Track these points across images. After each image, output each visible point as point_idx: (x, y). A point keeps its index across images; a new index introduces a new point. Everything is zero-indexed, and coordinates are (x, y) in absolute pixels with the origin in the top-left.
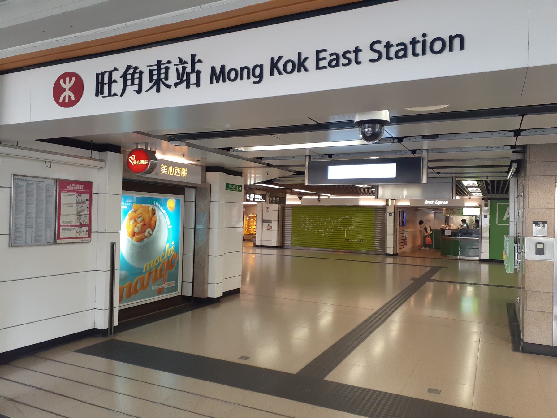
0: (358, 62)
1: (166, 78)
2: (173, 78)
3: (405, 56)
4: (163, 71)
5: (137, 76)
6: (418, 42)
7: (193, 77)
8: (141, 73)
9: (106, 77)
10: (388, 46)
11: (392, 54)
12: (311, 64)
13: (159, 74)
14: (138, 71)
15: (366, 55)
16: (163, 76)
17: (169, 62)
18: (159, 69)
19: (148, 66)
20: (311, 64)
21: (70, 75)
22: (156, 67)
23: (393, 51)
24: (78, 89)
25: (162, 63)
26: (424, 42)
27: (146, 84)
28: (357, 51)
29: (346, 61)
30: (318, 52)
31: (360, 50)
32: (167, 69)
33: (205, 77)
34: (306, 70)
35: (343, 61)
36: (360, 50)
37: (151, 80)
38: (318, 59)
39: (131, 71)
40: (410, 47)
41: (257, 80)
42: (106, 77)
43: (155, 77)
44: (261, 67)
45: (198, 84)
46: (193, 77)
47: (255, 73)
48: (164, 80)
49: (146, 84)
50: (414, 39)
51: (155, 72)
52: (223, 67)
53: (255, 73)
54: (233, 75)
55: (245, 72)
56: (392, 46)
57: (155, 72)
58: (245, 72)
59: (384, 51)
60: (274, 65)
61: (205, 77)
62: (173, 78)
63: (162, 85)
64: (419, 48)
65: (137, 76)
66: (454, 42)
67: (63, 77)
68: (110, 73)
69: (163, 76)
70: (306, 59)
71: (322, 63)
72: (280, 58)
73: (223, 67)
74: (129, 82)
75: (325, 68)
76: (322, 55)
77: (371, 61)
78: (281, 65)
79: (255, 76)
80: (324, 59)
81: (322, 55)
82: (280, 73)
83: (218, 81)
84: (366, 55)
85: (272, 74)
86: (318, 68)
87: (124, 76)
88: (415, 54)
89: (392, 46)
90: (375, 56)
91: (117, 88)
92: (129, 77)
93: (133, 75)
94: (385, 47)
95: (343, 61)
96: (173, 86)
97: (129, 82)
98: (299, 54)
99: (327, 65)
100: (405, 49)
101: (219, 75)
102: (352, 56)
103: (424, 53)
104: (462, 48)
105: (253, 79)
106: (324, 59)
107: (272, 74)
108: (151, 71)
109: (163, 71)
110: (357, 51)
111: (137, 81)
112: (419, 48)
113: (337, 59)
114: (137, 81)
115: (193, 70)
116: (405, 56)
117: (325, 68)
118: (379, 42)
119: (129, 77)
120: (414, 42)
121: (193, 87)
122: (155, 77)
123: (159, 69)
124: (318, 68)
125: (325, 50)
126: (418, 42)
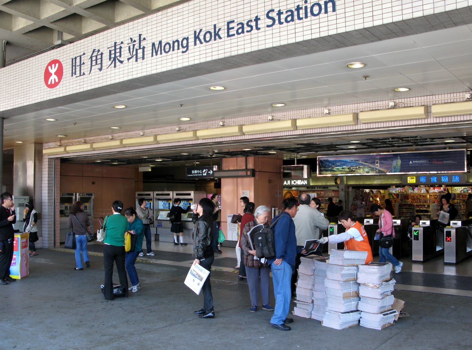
0: (258, 29)
1: (120, 56)
3: (292, 20)
4: (118, 51)
5: (99, 57)
6: (302, 8)
8: (102, 54)
9: (78, 60)
10: (280, 13)
11: (283, 20)
13: (115, 53)
14: (100, 53)
15: (264, 22)
16: (118, 54)
17: (122, 43)
18: (115, 50)
19: (108, 48)
22: (113, 48)
23: (283, 17)
25: (117, 44)
26: (306, 8)
27: (106, 61)
28: (257, 19)
29: (249, 29)
30: (228, 23)
31: (259, 19)
32: (121, 48)
34: (220, 38)
35: (247, 28)
36: (259, 19)
37: (110, 59)
38: (229, 29)
39: (95, 54)
40: (295, 13)
41: (185, 49)
42: (78, 60)
43: (113, 56)
44: (187, 39)
45: (143, 58)
46: (140, 52)
48: (118, 58)
49: (106, 61)
50: (298, 6)
51: (113, 52)
52: (160, 43)
55: (176, 44)
56: (282, 13)
57: (113, 52)
58: (176, 44)
59: (276, 18)
60: (196, 37)
63: (117, 61)
64: (302, 12)
65: (99, 57)
68: (80, 56)
69: (118, 54)
70: (219, 30)
71: (232, 32)
72: (201, 30)
73: (160, 43)
75: (234, 35)
76: (231, 25)
77: (268, 26)
78: (201, 37)
79: (183, 47)
80: (233, 28)
81: (231, 25)
82: (201, 43)
83: (156, 54)
84: (264, 22)
85: (195, 44)
86: (229, 36)
87: (91, 57)
88: (299, 18)
89: (282, 13)
90: (270, 22)
92: (94, 58)
93: (96, 56)
94: (277, 14)
95: (247, 28)
96: (126, 61)
98: (215, 26)
99: (236, 33)
100: (292, 15)
101: (158, 48)
102: (253, 24)
103: (306, 17)
104: (334, 10)
105: (181, 49)
106: (233, 28)
107: (195, 44)
108: (110, 51)
109: (118, 51)
110: (257, 19)
112: (302, 12)
113: (243, 28)
115: (140, 48)
116: (292, 20)
117: (234, 35)
118: (273, 11)
119: (94, 58)
120: (298, 8)
121: (140, 60)
122: (113, 56)
123: (115, 50)
124: (229, 36)
125: (233, 22)
126: (302, 8)
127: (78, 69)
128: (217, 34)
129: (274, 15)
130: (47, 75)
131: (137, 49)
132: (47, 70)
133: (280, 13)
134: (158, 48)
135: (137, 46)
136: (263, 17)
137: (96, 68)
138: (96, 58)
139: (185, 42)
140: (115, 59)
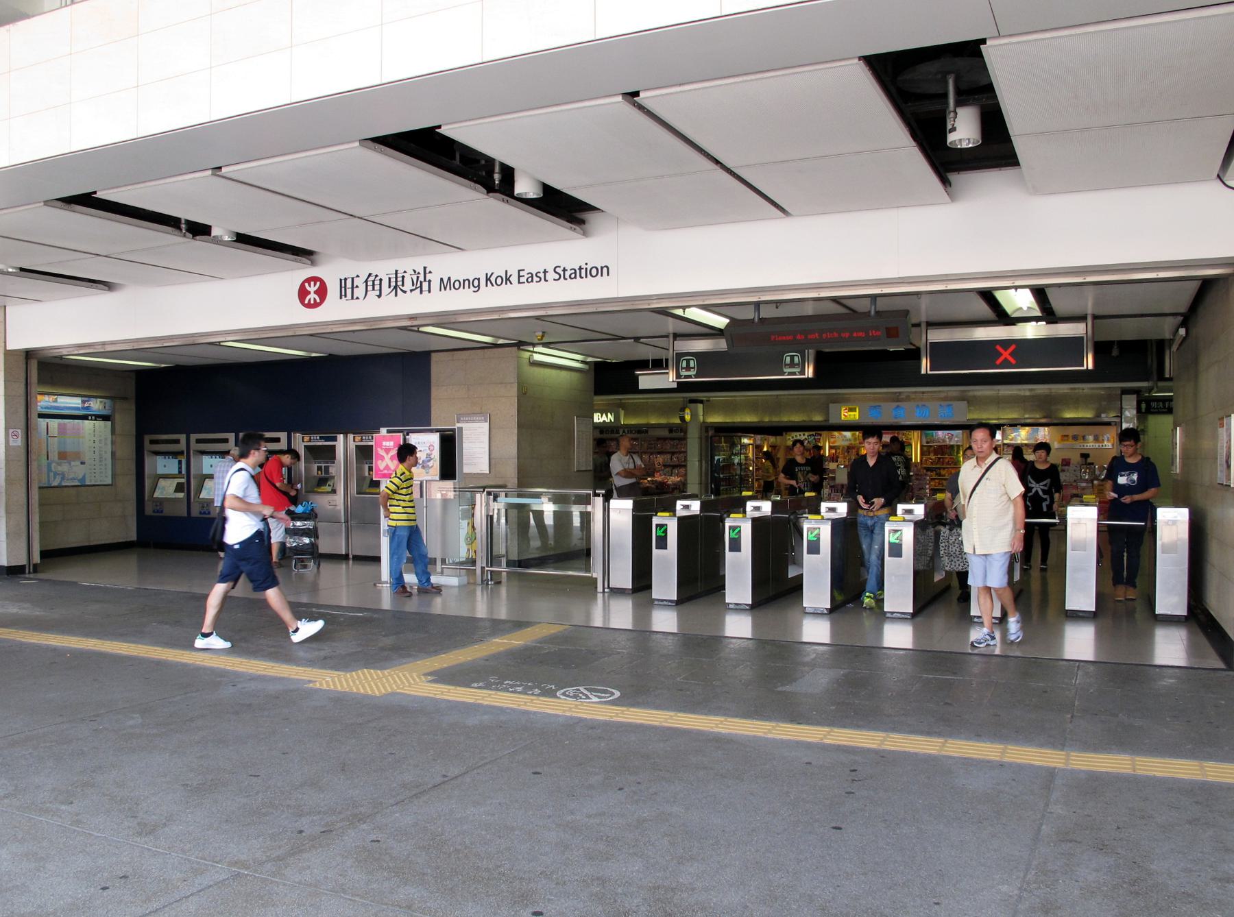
2: (408, 286)
5: (377, 282)
7: (425, 285)
10: (564, 270)
12: (514, 279)
15: (551, 275)
20: (514, 279)
21: (315, 279)
24: (322, 292)
33: (435, 285)
39: (372, 278)
46: (425, 285)
47: (474, 284)
51: (393, 280)
53: (474, 284)
54: (457, 285)
60: (488, 279)
61: (435, 285)
62: (408, 286)
65: (377, 282)
66: (603, 270)
67: (308, 280)
71: (522, 280)
74: (370, 288)
78: (493, 279)
84: (551, 275)
87: (366, 281)
91: (359, 292)
92: (370, 283)
95: (535, 279)
97: (370, 288)
101: (446, 284)
102: (542, 275)
110: (545, 272)
111: (377, 287)
114: (377, 287)
119: (370, 283)
120: (580, 268)
121: (425, 293)
122: (393, 284)
127: (349, 291)
128: (508, 279)
129: (559, 270)
130: (303, 293)
131: (422, 283)
132: (302, 285)
133: (564, 270)
134: (446, 284)
135: (422, 278)
136: (551, 270)
137: (372, 294)
138: (372, 283)
139: (476, 283)
140: (395, 287)
